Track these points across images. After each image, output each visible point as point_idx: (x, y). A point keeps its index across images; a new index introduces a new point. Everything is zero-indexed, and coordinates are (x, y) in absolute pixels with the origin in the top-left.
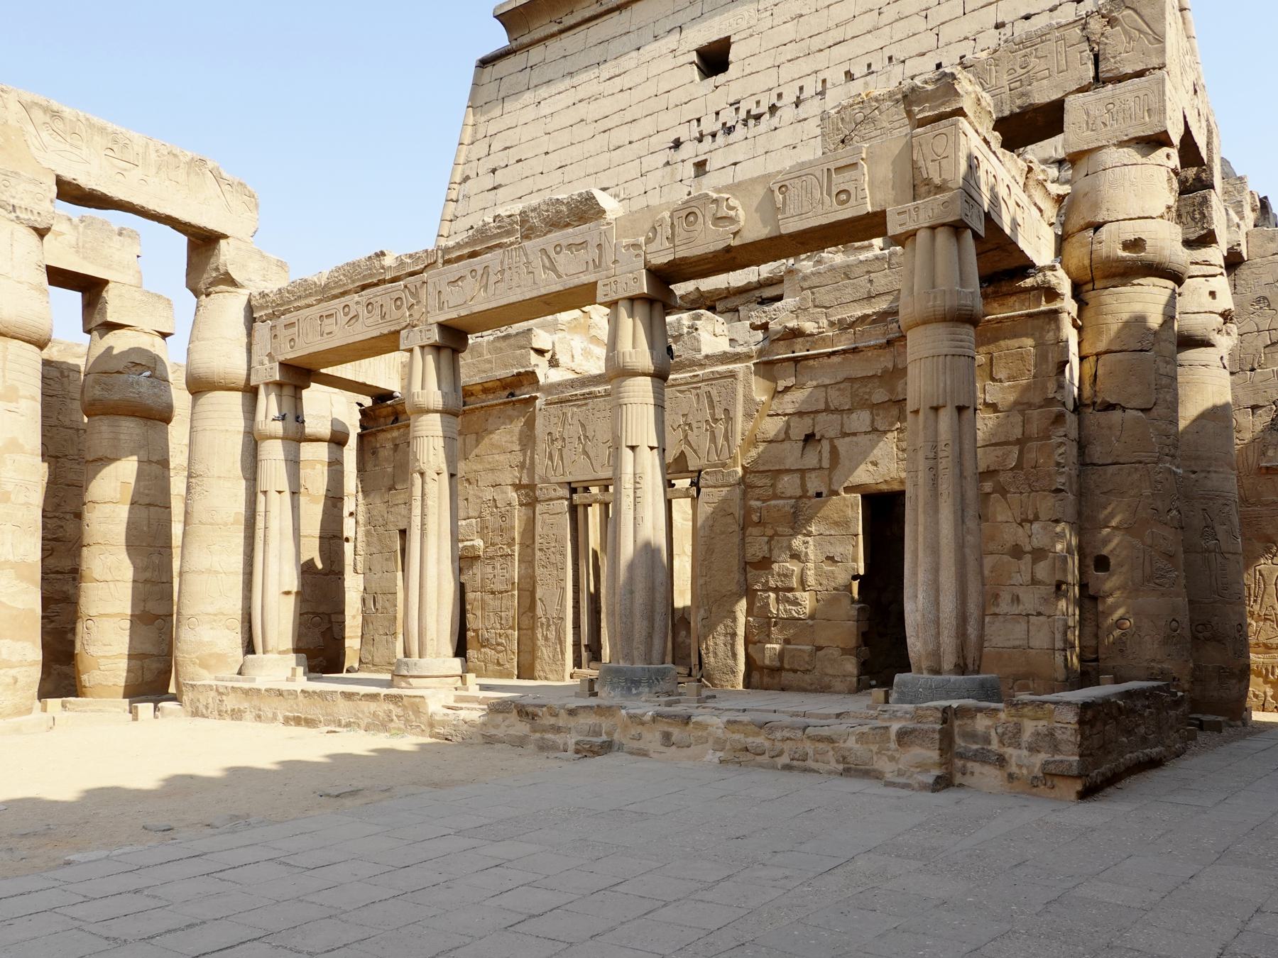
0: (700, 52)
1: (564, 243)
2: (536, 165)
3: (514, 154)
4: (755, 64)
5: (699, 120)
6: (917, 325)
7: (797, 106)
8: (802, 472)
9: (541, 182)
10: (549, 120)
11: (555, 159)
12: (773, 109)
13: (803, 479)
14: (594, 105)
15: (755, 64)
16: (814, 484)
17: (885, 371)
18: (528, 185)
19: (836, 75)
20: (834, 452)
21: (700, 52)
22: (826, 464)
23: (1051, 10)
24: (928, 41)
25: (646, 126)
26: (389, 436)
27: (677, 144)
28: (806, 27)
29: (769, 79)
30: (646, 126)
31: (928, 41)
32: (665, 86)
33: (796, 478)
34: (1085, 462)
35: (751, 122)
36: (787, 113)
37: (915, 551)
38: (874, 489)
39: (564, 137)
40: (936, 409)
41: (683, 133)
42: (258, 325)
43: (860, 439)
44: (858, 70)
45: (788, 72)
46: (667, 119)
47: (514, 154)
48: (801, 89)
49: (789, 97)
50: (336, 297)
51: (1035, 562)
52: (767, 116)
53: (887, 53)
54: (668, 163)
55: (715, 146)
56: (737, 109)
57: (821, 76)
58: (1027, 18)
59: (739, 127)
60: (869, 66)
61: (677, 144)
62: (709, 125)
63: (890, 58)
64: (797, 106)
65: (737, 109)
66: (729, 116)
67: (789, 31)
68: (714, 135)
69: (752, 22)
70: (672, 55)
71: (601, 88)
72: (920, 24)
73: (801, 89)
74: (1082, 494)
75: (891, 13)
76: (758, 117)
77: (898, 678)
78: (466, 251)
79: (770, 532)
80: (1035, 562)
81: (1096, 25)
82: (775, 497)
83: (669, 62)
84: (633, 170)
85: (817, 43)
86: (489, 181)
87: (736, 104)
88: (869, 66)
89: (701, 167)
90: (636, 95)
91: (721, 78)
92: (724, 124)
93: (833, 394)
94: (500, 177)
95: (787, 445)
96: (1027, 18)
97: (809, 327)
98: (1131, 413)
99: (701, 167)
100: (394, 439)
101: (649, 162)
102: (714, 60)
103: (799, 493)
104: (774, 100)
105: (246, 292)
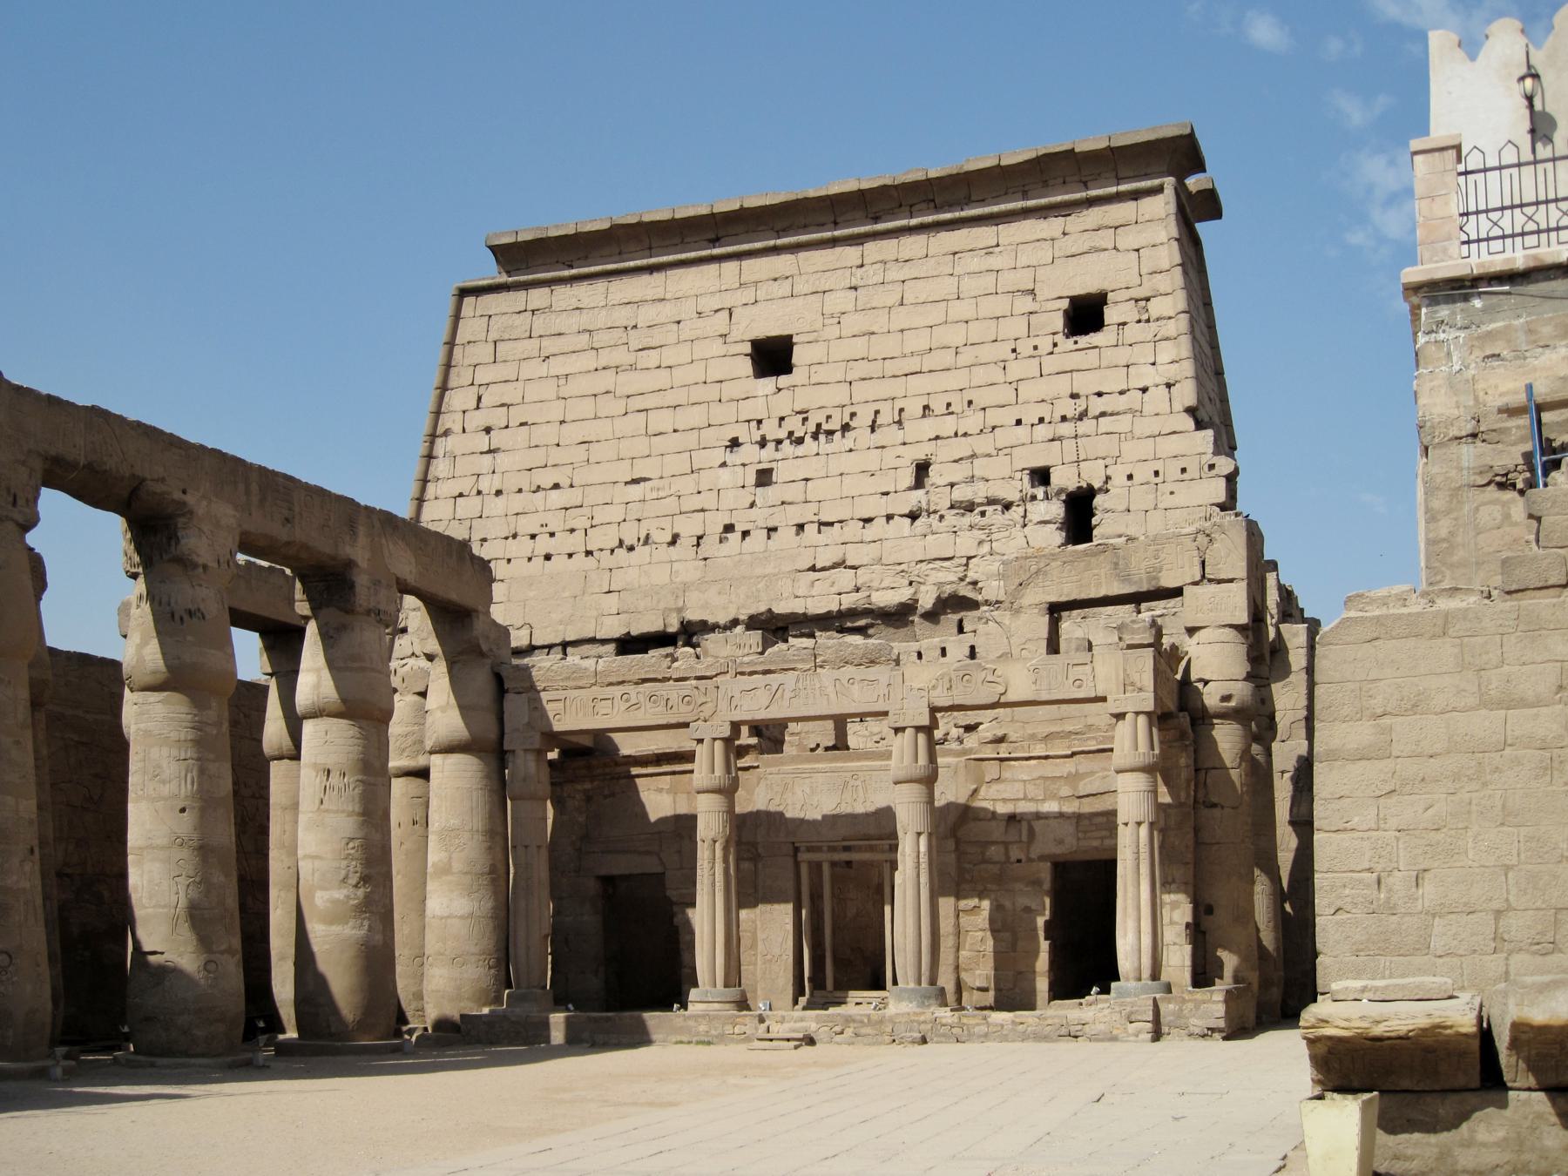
0: (756, 344)
1: (858, 678)
2: (546, 434)
3: (517, 415)
4: (821, 374)
5: (760, 422)
6: (1132, 770)
7: (873, 431)
8: (1006, 844)
9: (556, 456)
10: (562, 381)
11: (572, 433)
12: (846, 428)
13: (1007, 850)
14: (622, 377)
15: (821, 374)
16: (1015, 853)
17: (1069, 774)
18: (537, 457)
19: (913, 408)
20: (1032, 833)
21: (756, 344)
22: (1024, 838)
23: (1122, 393)
24: (1007, 394)
25: (695, 416)
26: (579, 787)
27: (735, 443)
29: (839, 394)
30: (695, 416)
31: (1007, 394)
32: (714, 375)
33: (1001, 849)
34: (1198, 843)
35: (822, 437)
36: (861, 435)
37: (1125, 909)
38: (1061, 859)
40: (1139, 824)
41: (741, 432)
42: (509, 697)
43: (1051, 822)
44: (938, 407)
45: (862, 391)
46: (720, 413)
47: (517, 415)
48: (877, 412)
49: (864, 419)
50: (611, 684)
51: (1172, 909)
52: (838, 434)
53: (967, 396)
54: (724, 465)
55: (779, 456)
56: (805, 420)
57: (899, 404)
58: (1100, 394)
59: (808, 439)
60: (949, 405)
61: (735, 443)
62: (772, 430)
63: (970, 402)
64: (873, 431)
65: (805, 420)
66: (794, 424)
67: (859, 347)
68: (779, 442)
69: (818, 325)
70: (721, 340)
71: (630, 358)
72: (998, 376)
73: (877, 412)
74: (1197, 863)
75: (966, 357)
76: (830, 433)
77: (1114, 985)
78: (760, 668)
79: (980, 887)
80: (1172, 909)
81: (1202, 539)
82: (984, 861)
83: (717, 348)
84: (680, 464)
86: (483, 442)
87: (804, 414)
88: (949, 405)
89: (764, 478)
91: (783, 380)
92: (791, 434)
93: (1030, 787)
94: (497, 439)
95: (994, 823)
96: (1100, 394)
97: (1013, 736)
98: (1227, 810)
99: (764, 478)
100: (585, 791)
101: (700, 459)
102: (772, 357)
103: (1003, 859)
104: (847, 419)
105: (489, 661)
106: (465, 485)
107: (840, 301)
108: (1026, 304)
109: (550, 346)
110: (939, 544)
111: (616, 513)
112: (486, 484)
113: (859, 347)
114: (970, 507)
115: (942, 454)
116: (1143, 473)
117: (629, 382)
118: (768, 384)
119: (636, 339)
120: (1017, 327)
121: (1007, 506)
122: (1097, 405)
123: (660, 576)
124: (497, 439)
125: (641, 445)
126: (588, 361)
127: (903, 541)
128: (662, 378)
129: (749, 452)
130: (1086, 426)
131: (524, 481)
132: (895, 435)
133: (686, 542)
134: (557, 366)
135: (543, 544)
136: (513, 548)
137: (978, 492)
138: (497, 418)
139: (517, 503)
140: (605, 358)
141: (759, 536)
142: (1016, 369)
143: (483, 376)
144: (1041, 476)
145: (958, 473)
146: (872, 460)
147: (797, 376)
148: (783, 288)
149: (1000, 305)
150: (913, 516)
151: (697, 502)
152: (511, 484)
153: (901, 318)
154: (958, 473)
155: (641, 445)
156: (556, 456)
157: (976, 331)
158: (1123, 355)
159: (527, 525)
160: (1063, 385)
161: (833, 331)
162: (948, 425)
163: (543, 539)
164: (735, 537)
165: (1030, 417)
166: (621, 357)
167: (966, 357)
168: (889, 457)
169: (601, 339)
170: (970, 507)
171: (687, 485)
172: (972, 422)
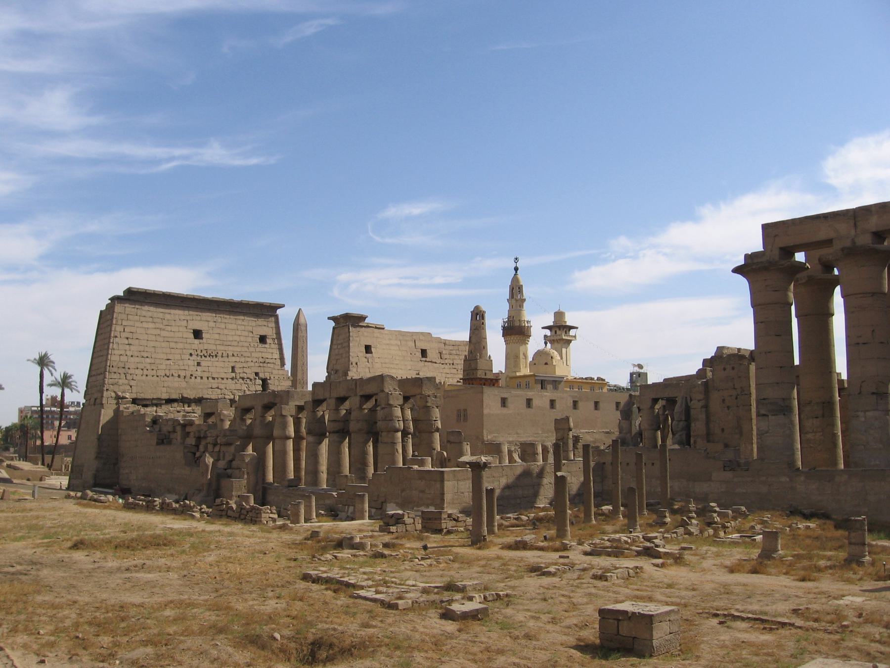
2: (144, 343)
3: (135, 336)
9: (146, 349)
12: (216, 356)
18: (142, 349)
28: (223, 338)
39: (153, 338)
46: (188, 346)
49: (220, 354)
66: (204, 352)
67: (217, 336)
75: (241, 344)
83: (185, 330)
85: (225, 343)
90: (177, 335)
99: (199, 364)
102: (197, 334)
106: (123, 352)
107: (212, 324)
108: (251, 335)
109: (143, 319)
110: (238, 386)
111: (163, 367)
112: (129, 353)
113: (217, 336)
114: (243, 379)
115: (238, 365)
116: (277, 377)
117: (163, 333)
118: (197, 341)
119: (165, 322)
120: (250, 340)
121: (251, 380)
122: (267, 361)
123: (176, 385)
124: (130, 341)
125: (168, 351)
126: (151, 325)
127: (231, 385)
128: (172, 334)
129: (194, 357)
130: (265, 365)
131: (138, 354)
132: (226, 359)
133: (182, 377)
134: (145, 325)
135: (145, 372)
136: (137, 372)
137: (245, 376)
138: (130, 335)
139: (137, 360)
140: (158, 325)
141: (199, 378)
142: (252, 349)
143: (124, 323)
144: (257, 374)
145: (241, 371)
146: (222, 364)
147: (204, 340)
148: (199, 318)
149: (246, 334)
150: (232, 379)
151: (183, 368)
152: (136, 354)
153: (226, 332)
154: (241, 371)
155: (168, 351)
156: (146, 349)
157: (242, 339)
158: (271, 351)
159: (140, 366)
160: (260, 355)
161: (211, 331)
162: (238, 359)
163: (145, 371)
164: (193, 378)
165: (255, 360)
166: (161, 326)
167: (241, 344)
168: (226, 364)
169: (155, 320)
170: (243, 379)
171: (181, 363)
172: (243, 359)
